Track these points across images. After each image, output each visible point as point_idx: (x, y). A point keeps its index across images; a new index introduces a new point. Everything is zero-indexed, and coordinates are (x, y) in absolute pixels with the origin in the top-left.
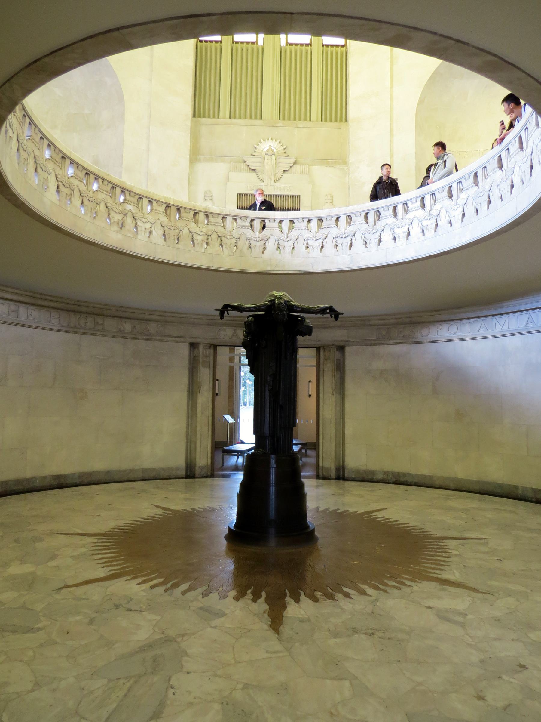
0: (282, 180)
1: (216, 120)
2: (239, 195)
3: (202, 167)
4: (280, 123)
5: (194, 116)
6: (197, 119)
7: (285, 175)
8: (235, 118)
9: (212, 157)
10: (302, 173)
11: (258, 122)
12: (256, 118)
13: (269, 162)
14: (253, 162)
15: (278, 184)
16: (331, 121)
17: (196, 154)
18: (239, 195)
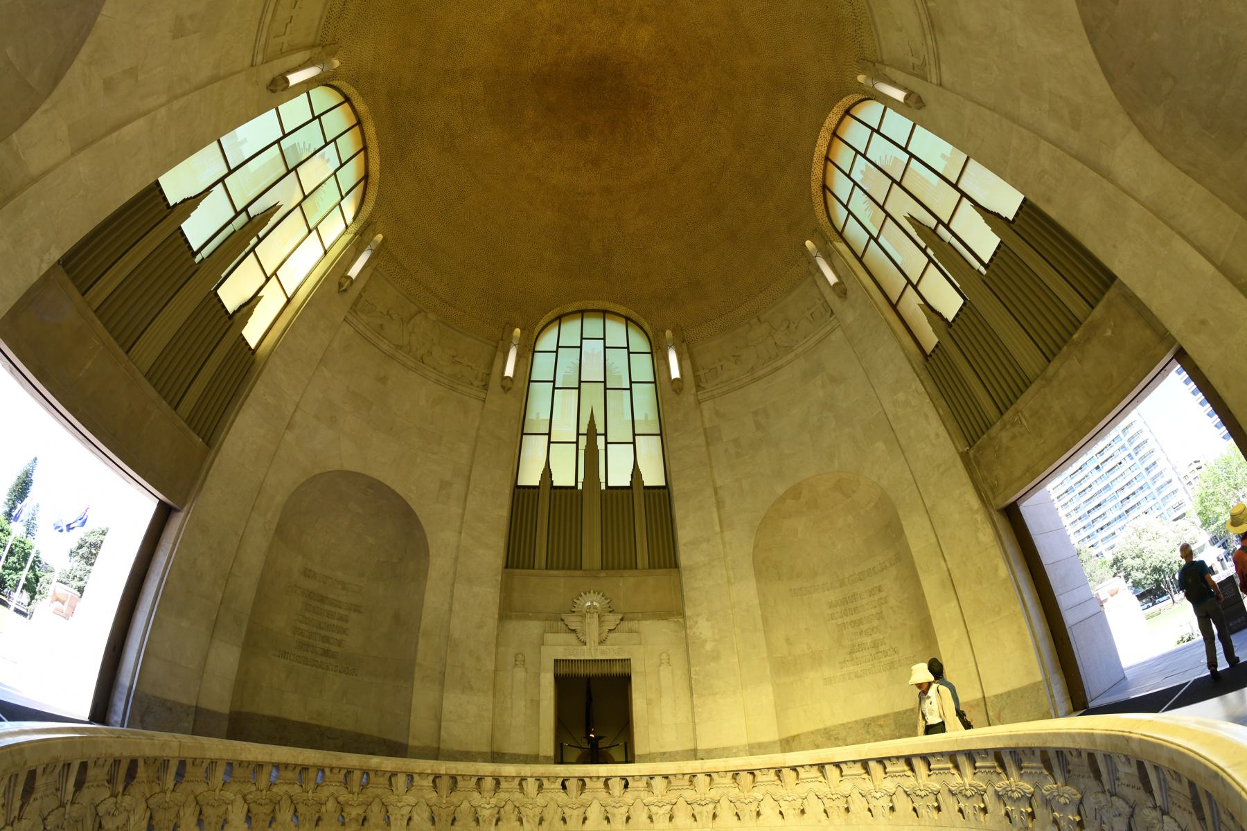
0: (608, 642)
1: (531, 571)
2: (556, 661)
3: (514, 626)
4: (603, 574)
5: (507, 567)
6: (510, 570)
7: (612, 635)
8: (552, 569)
9: (524, 615)
10: (631, 631)
11: (578, 573)
12: (575, 569)
13: (592, 622)
14: (573, 622)
15: (603, 647)
16: (660, 568)
17: (508, 610)
18: (556, 661)
